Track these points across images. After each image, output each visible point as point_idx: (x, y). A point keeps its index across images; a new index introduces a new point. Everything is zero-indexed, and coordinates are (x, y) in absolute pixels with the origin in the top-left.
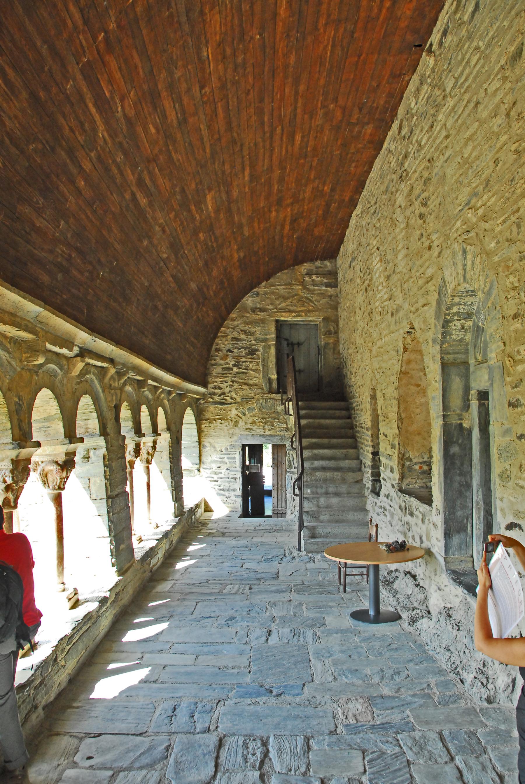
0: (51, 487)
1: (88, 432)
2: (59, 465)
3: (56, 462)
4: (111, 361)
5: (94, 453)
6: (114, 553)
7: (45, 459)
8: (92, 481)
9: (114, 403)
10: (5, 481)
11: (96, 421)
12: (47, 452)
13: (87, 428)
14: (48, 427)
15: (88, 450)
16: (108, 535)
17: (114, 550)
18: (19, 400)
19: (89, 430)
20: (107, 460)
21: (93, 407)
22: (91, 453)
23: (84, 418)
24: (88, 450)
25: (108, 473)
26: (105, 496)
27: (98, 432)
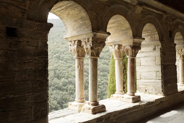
0: (129, 55)
1: (155, 39)
2: (131, 47)
3: (130, 46)
4: (165, 12)
5: (157, 47)
6: (163, 87)
7: (127, 44)
8: (156, 58)
9: (169, 30)
10: (90, 45)
11: (158, 35)
12: (127, 42)
13: (155, 38)
14: (128, 32)
15: (155, 47)
16: (161, 79)
17: (163, 85)
18: (97, 14)
19: (156, 39)
20: (162, 50)
21: (156, 29)
22: (156, 47)
23: (153, 34)
24: (155, 47)
25: (162, 55)
26: (160, 64)
27: (159, 39)
